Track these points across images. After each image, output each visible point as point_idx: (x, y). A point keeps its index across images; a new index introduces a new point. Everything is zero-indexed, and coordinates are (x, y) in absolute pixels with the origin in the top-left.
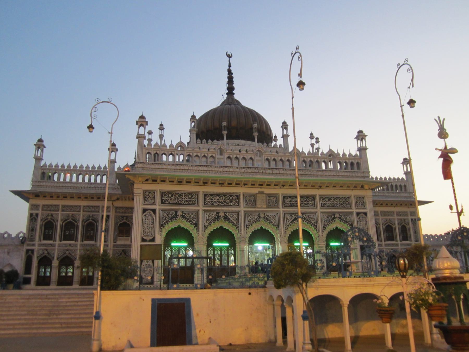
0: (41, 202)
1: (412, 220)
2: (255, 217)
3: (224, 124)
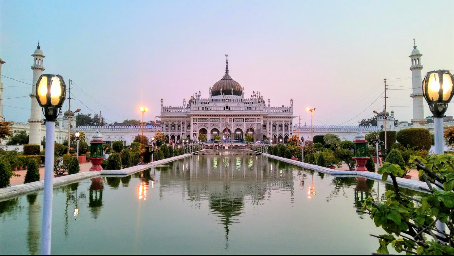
0: (164, 119)
1: (290, 123)
3: (221, 90)
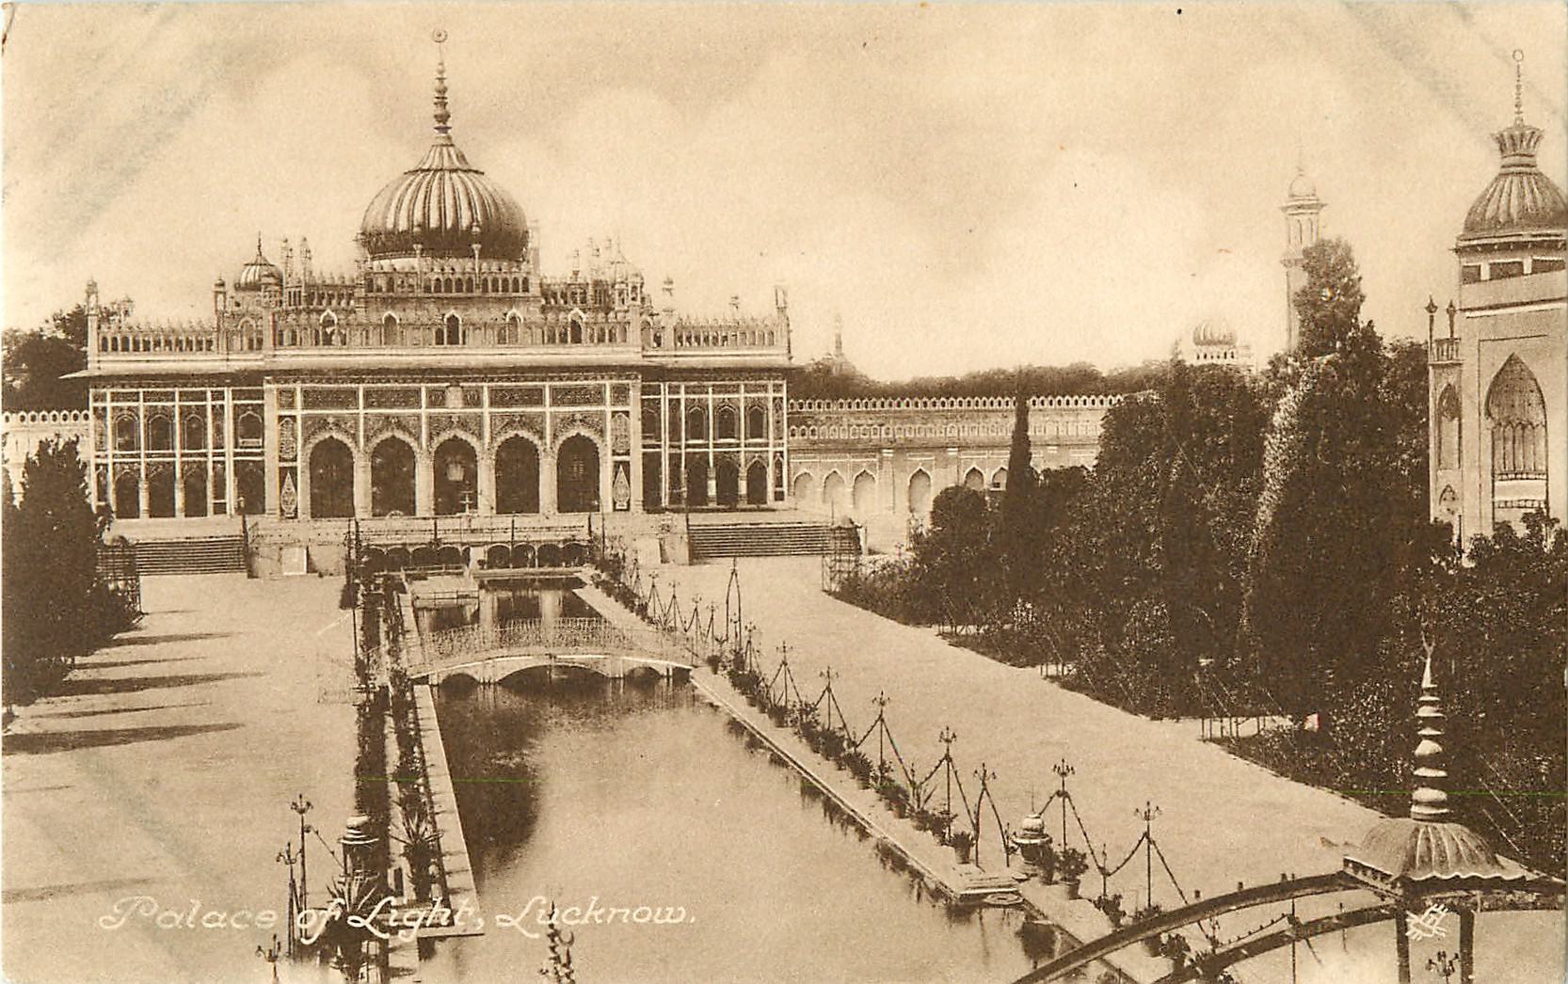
2: (444, 422)
